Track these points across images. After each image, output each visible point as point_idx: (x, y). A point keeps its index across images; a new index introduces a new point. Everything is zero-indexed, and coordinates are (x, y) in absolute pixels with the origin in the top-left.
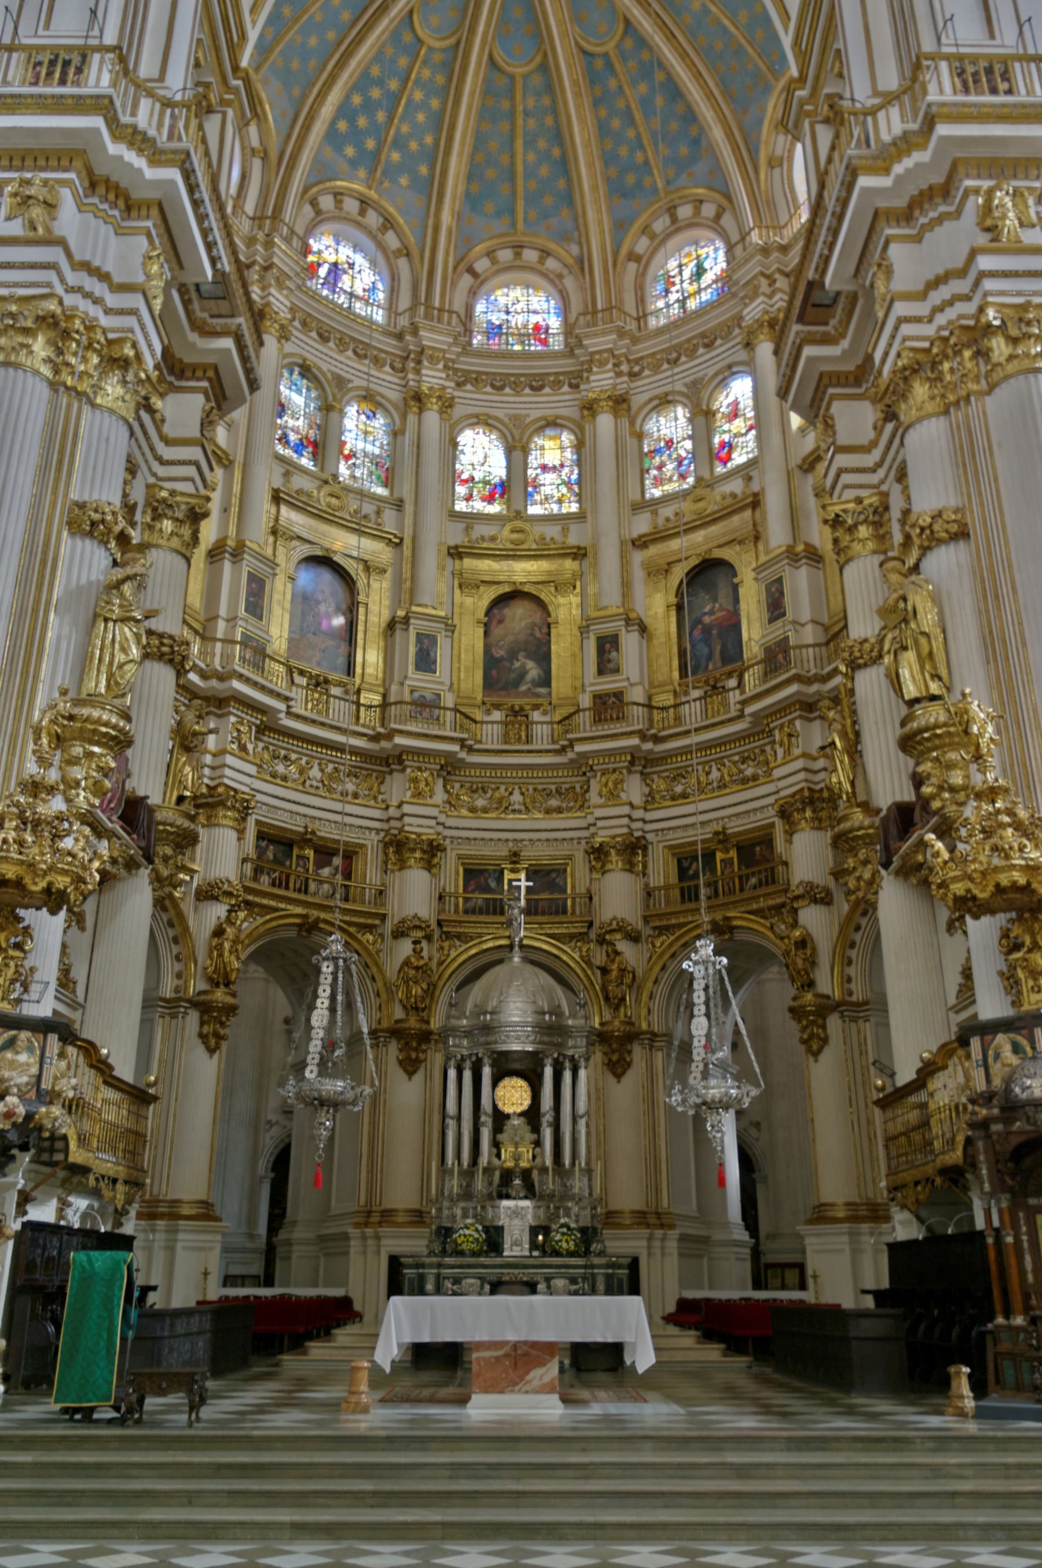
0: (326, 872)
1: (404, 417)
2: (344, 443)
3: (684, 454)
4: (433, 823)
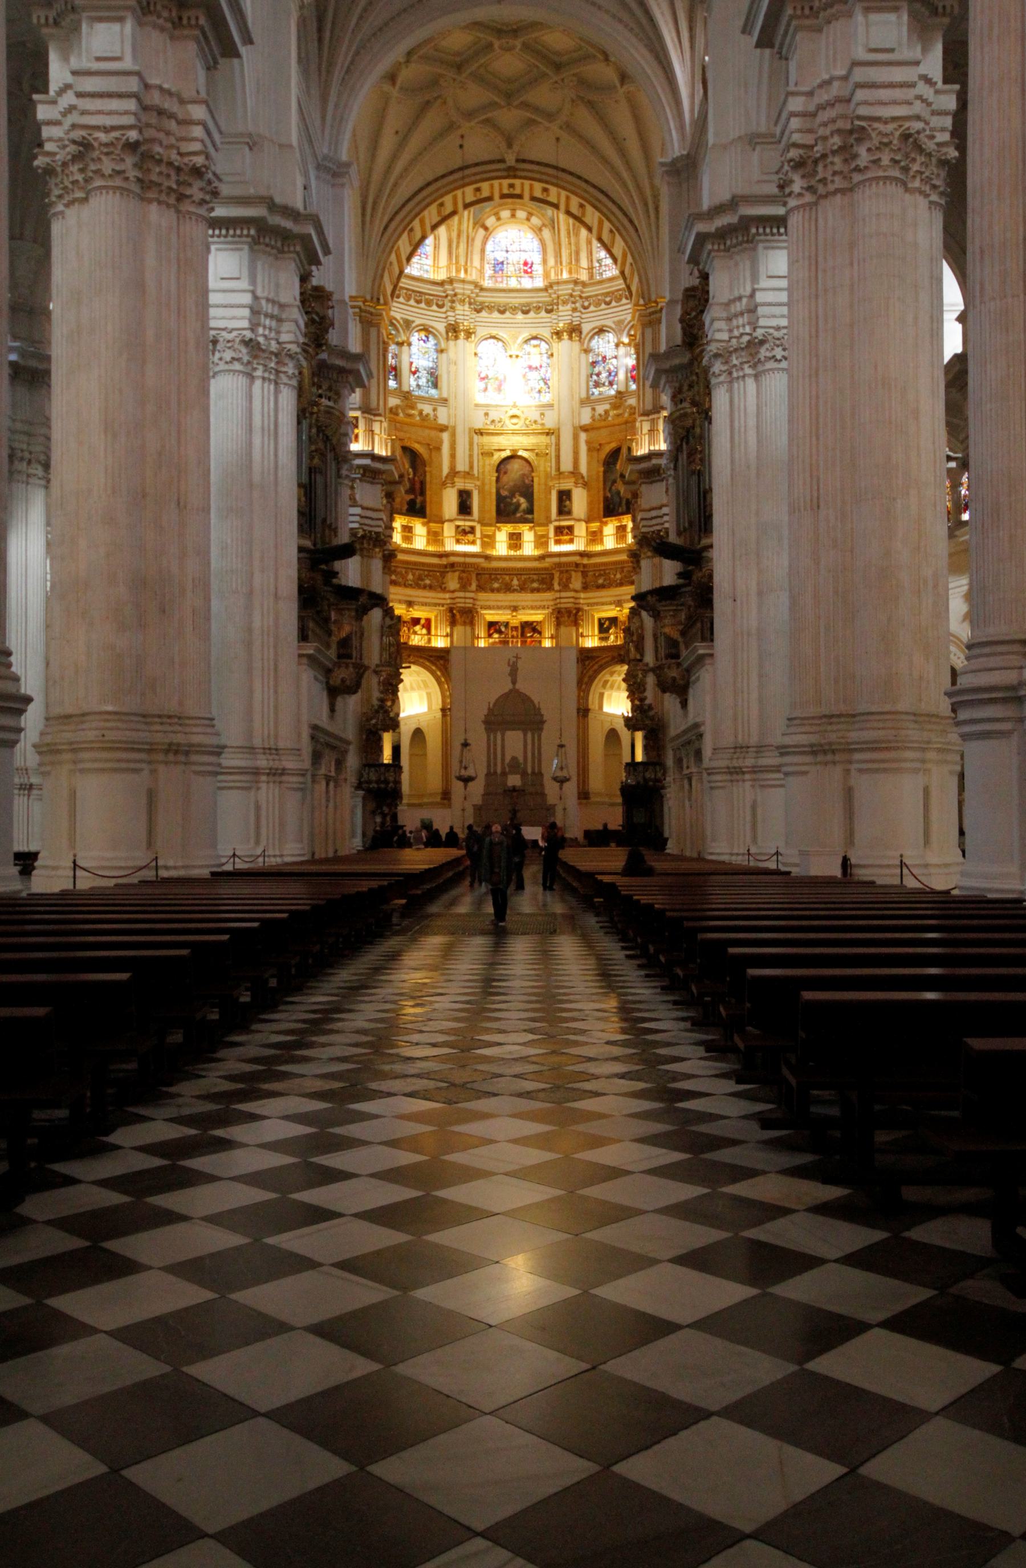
0: (417, 628)
1: (447, 339)
2: (411, 363)
3: (612, 368)
4: (471, 601)
